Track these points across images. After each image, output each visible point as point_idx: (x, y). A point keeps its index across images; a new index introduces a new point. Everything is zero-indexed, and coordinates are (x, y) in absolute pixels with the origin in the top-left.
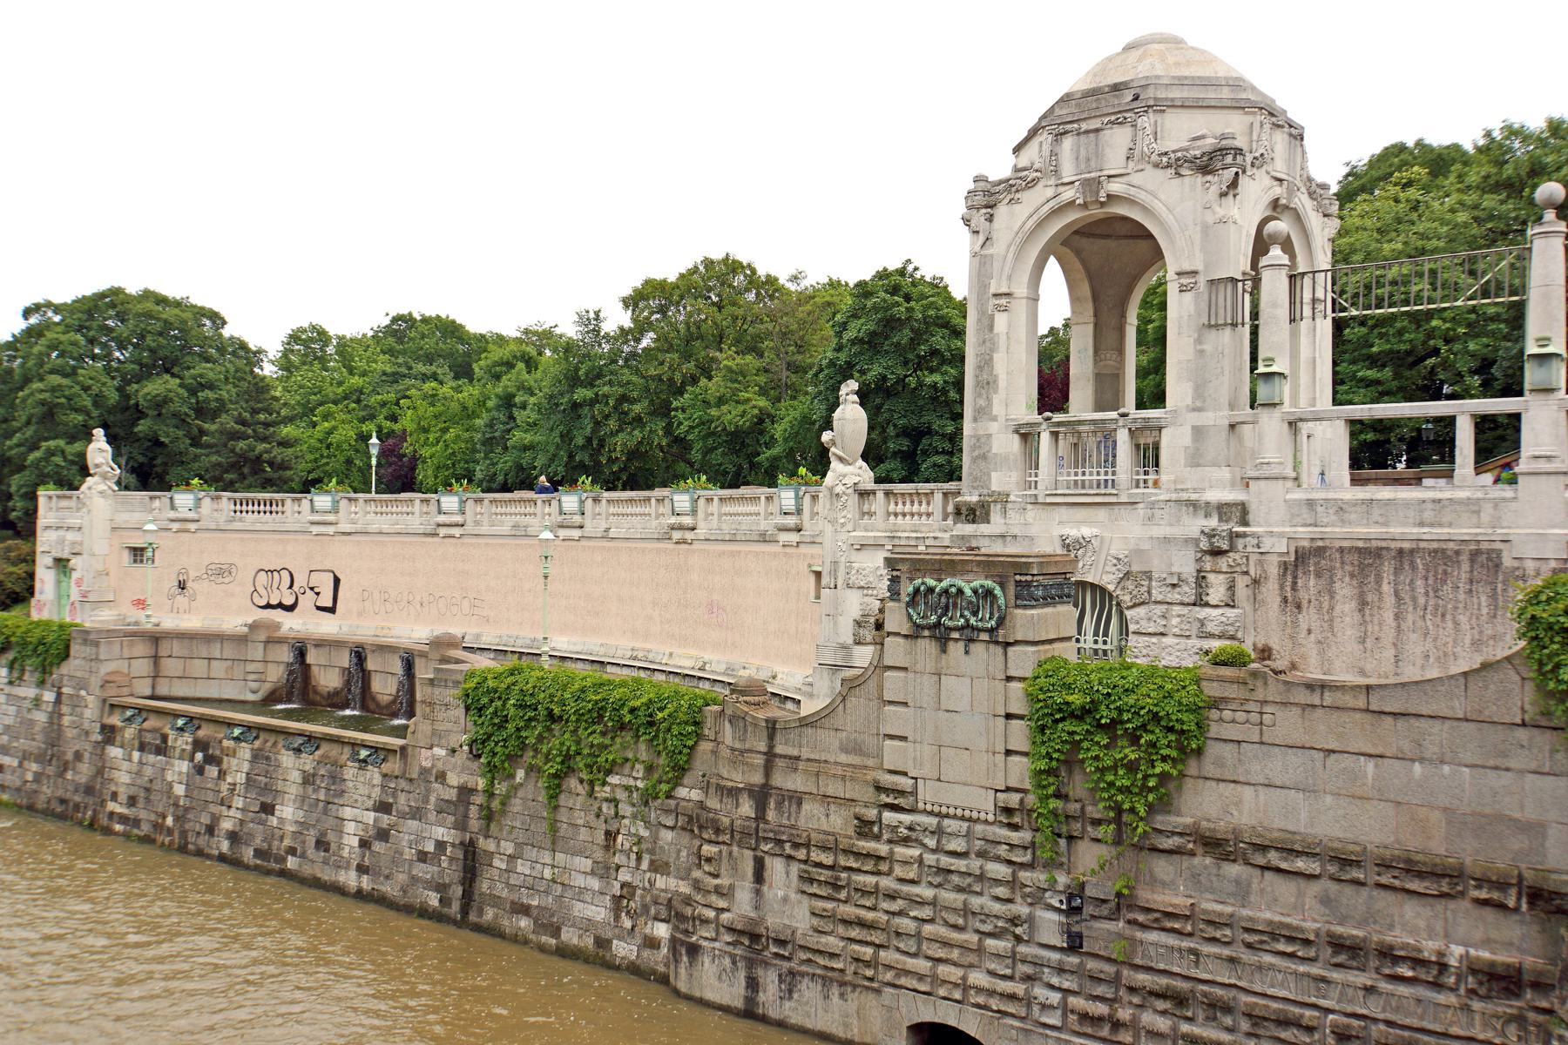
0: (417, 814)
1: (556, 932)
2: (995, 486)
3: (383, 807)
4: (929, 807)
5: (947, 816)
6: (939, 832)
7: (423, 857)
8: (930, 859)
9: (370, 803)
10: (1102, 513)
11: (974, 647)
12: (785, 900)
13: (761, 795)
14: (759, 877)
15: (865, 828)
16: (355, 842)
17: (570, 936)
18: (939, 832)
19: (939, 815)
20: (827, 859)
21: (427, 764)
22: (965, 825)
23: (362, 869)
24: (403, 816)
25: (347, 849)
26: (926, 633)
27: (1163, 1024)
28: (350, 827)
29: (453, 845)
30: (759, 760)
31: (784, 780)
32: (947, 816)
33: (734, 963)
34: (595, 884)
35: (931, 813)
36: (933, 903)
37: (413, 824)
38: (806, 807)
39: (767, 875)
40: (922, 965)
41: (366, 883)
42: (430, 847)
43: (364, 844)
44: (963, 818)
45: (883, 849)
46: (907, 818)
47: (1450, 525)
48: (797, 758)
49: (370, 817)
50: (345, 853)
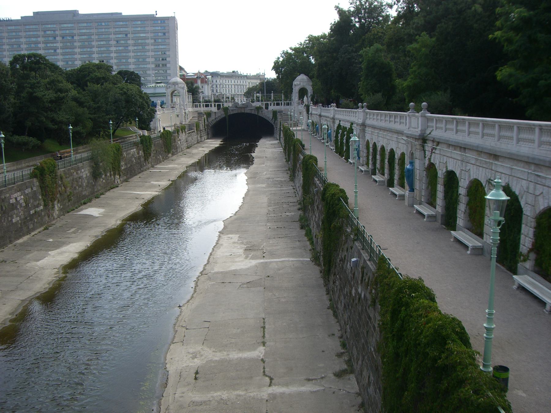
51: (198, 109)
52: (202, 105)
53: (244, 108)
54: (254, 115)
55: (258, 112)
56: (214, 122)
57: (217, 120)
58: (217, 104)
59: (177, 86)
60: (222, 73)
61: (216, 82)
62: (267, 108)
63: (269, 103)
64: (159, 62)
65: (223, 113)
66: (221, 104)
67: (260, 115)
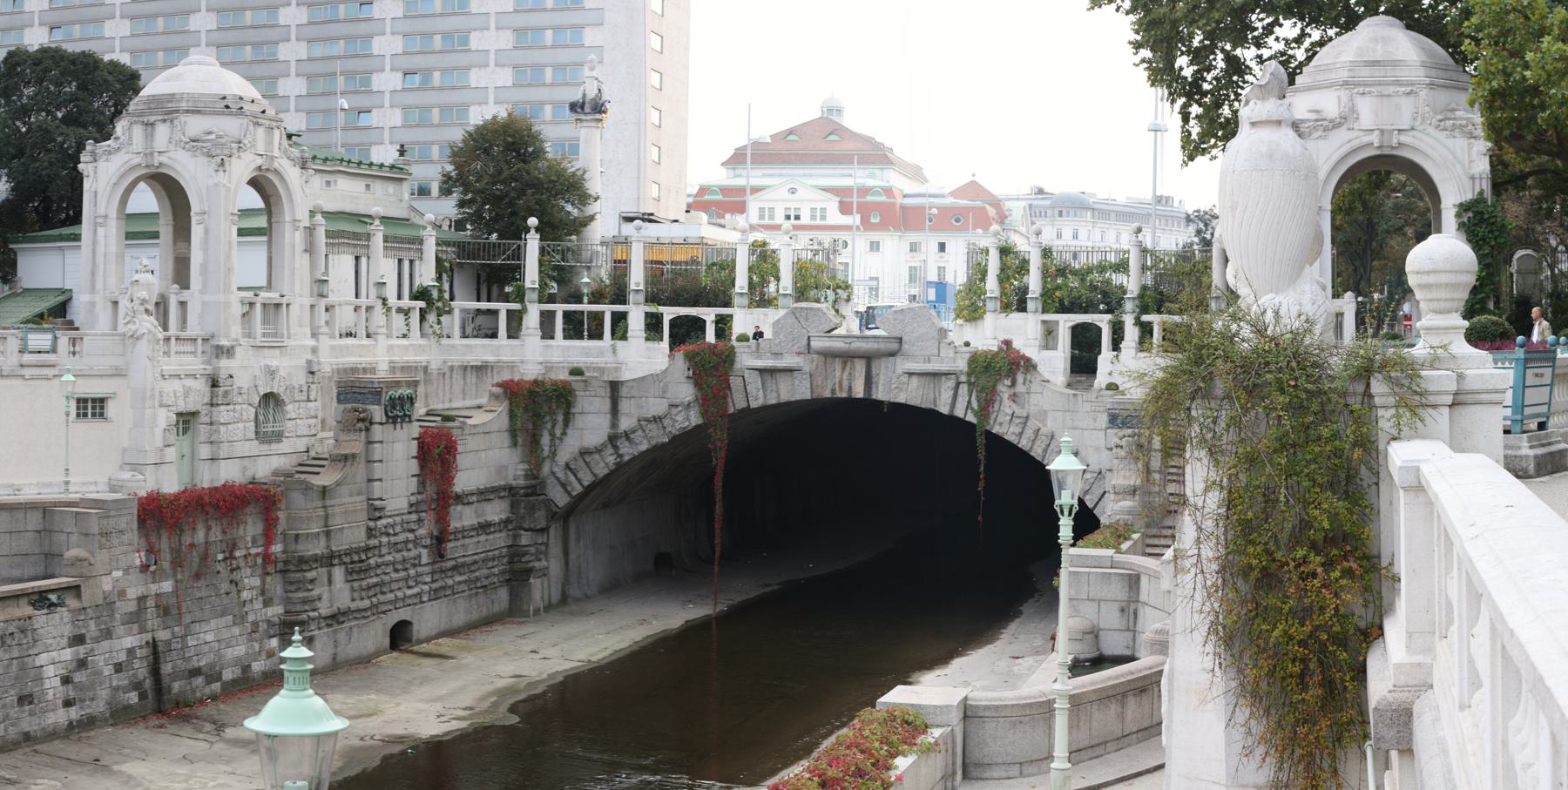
0: (107, 634)
1: (219, 677)
3: (78, 640)
7: (119, 668)
8: (392, 539)
9: (65, 642)
10: (277, 351)
14: (330, 582)
15: (370, 532)
16: (57, 682)
17: (228, 675)
18: (392, 526)
21: (108, 587)
23: (68, 703)
24: (96, 640)
25: (51, 692)
27: (450, 582)
28: (50, 671)
29: (141, 647)
34: (236, 631)
36: (393, 563)
37: (106, 644)
40: (391, 596)
41: (74, 713)
42: (123, 657)
43: (66, 680)
46: (384, 522)
49: (68, 654)
50: (50, 697)
51: (497, 350)
52: (532, 319)
53: (869, 358)
54: (951, 419)
55: (987, 405)
56: (604, 465)
57: (628, 451)
58: (669, 313)
59: (162, 131)
60: (1106, 202)
61: (1075, 237)
62: (1083, 364)
63: (1103, 321)
64: (537, 57)
65: (686, 392)
66: (709, 315)
67: (1004, 425)
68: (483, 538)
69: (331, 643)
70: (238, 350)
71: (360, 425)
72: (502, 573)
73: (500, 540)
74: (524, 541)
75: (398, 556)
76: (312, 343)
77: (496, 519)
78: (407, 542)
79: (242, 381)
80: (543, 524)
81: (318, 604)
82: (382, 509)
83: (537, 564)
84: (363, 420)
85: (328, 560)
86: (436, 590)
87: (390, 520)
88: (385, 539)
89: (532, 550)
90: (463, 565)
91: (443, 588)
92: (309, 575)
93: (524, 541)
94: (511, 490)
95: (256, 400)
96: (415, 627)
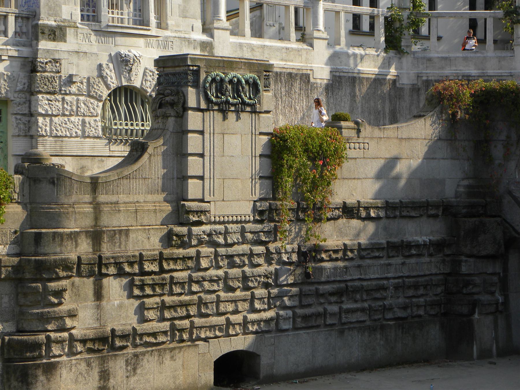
2: (65, 16)
4: (217, 219)
5: (228, 222)
6: (227, 232)
8: (222, 251)
11: (243, 115)
12: (120, 306)
13: (96, 236)
14: (98, 295)
19: (223, 223)
20: (154, 267)
22: (239, 225)
26: (216, 108)
30: (88, 209)
31: (112, 221)
32: (228, 222)
33: (89, 365)
35: (220, 223)
38: (132, 235)
39: (104, 292)
44: (237, 222)
45: (192, 252)
46: (207, 228)
47: (292, 61)
48: (117, 203)
68: (399, 260)
69: (95, 373)
70: (70, 32)
71: (170, 111)
72: (432, 304)
73: (429, 266)
74: (464, 269)
75: (235, 272)
76: (205, 38)
77: (421, 239)
78: (251, 255)
79: (82, 69)
80: (490, 250)
81: (69, 323)
82: (203, 212)
83: (485, 298)
84: (172, 104)
85: (96, 270)
86: (305, 318)
87: (220, 228)
88: (206, 250)
89: (477, 280)
90: (356, 290)
91: (318, 315)
92: (53, 285)
93: (464, 269)
94: (445, 210)
95: (105, 93)
96: (265, 361)
